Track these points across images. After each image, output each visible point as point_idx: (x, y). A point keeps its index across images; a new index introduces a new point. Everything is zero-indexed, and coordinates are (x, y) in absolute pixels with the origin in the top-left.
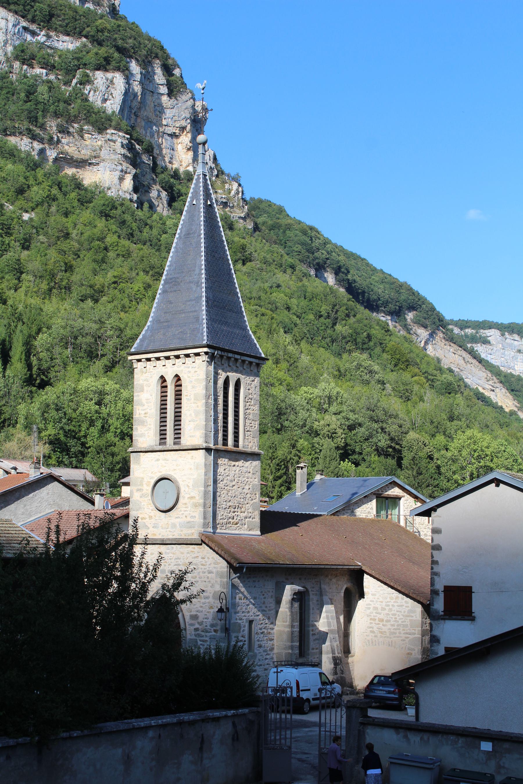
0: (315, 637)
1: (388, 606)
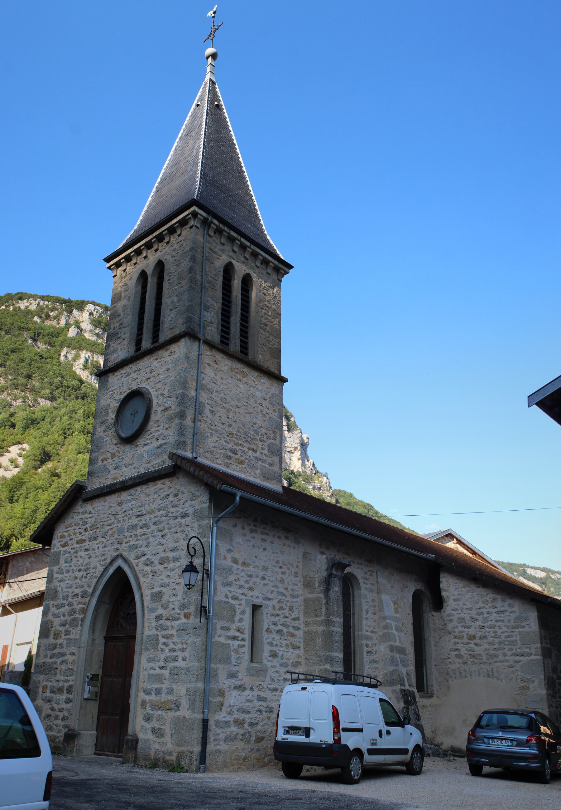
0: (372, 657)
1: (482, 614)
